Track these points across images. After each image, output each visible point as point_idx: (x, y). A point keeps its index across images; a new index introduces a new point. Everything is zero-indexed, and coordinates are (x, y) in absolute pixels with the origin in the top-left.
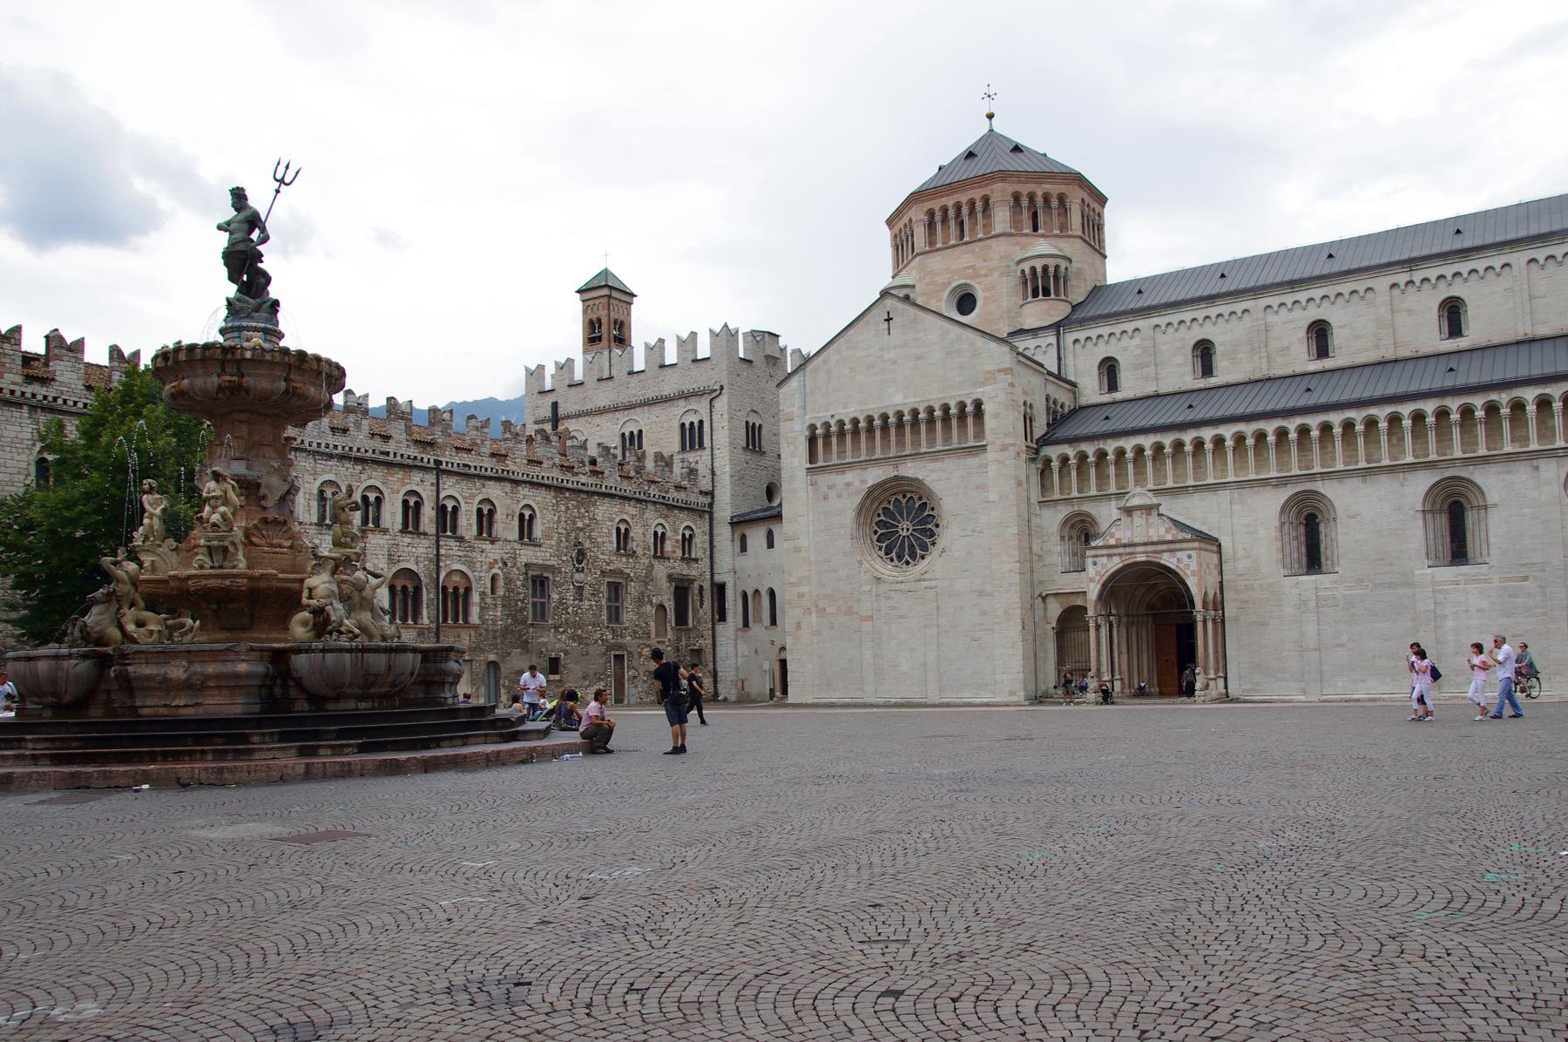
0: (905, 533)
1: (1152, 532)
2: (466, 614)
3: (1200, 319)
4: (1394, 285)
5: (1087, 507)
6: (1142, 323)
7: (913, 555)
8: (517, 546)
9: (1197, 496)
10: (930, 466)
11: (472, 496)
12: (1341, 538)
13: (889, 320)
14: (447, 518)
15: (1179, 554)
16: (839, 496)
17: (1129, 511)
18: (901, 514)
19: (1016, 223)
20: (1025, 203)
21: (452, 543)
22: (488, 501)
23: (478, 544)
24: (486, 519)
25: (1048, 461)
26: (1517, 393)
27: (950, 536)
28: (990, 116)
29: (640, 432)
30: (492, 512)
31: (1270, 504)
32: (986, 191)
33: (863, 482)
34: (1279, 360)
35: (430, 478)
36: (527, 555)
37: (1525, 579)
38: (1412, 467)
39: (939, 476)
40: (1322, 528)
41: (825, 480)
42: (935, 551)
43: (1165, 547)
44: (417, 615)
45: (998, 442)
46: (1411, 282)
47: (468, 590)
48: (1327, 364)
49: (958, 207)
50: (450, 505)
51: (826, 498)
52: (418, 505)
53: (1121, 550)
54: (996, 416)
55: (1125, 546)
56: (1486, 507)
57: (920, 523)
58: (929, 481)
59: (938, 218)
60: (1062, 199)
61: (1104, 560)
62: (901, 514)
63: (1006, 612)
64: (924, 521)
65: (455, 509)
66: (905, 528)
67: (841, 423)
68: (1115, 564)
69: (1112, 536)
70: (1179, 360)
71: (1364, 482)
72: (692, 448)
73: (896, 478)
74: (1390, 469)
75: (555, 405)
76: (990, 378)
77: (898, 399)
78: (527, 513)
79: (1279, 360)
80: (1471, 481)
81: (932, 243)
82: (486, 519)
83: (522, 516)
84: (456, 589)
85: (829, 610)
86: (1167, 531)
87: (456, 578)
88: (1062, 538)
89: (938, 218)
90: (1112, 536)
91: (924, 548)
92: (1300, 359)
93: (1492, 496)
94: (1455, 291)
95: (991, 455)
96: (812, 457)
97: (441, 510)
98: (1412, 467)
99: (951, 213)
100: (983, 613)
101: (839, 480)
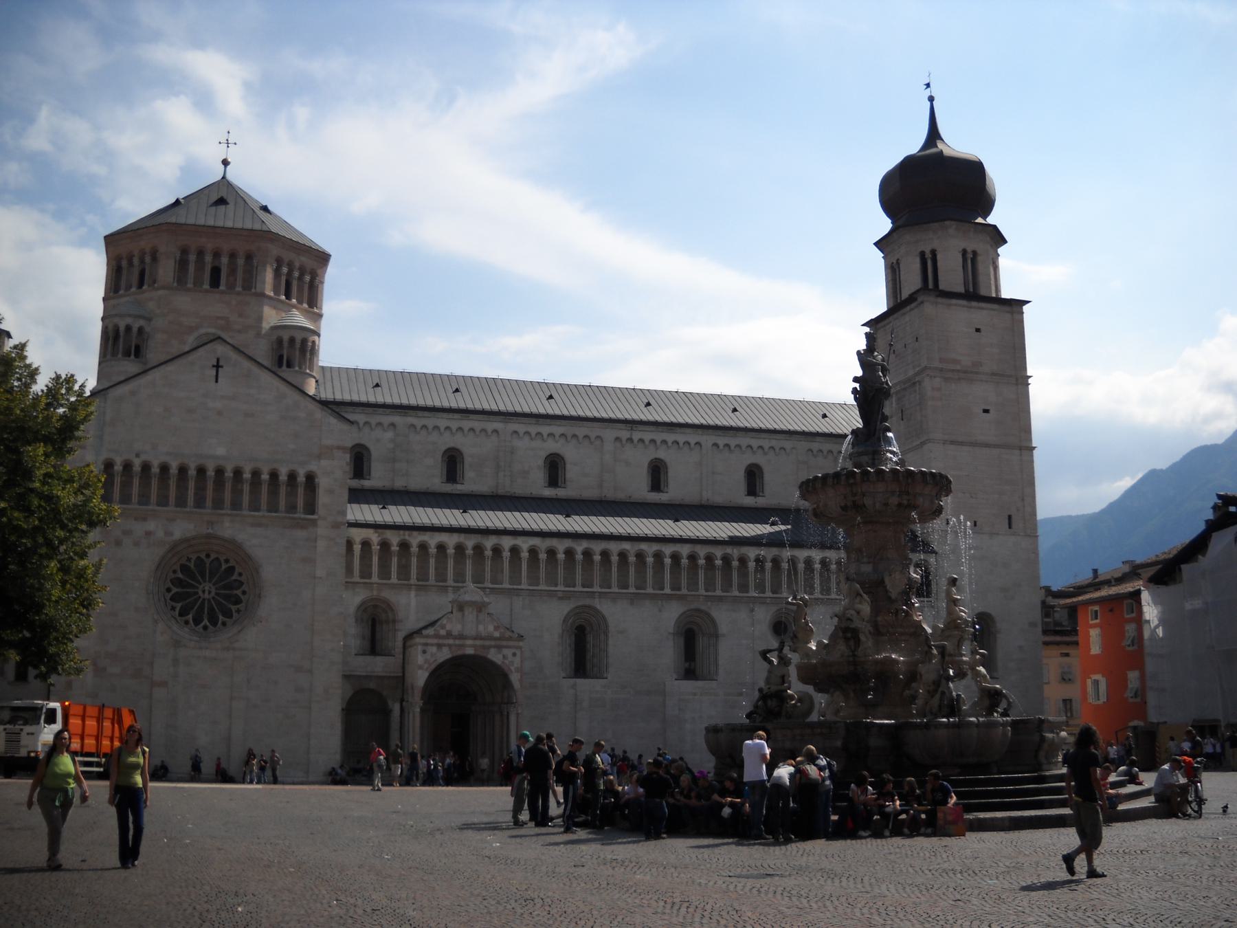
0: (206, 596)
1: (481, 628)
3: (454, 428)
4: (617, 439)
5: (387, 594)
6: (397, 419)
13: (217, 366)
15: (505, 651)
16: (137, 544)
18: (203, 576)
19: (276, 289)
20: (285, 270)
25: (350, 544)
28: (225, 163)
37: (741, 694)
38: (669, 597)
40: (590, 638)
43: (493, 643)
46: (630, 440)
49: (217, 255)
51: (118, 543)
53: (451, 641)
54: (331, 492)
55: (455, 638)
59: (192, 258)
61: (434, 649)
62: (203, 576)
66: (207, 590)
67: (146, 467)
68: (445, 655)
71: (632, 604)
73: (209, 536)
74: (653, 597)
77: (219, 450)
80: (708, 615)
81: (181, 278)
86: (496, 628)
88: (356, 621)
89: (192, 258)
90: (443, 627)
93: (723, 628)
94: (662, 454)
95: (322, 530)
99: (208, 258)
101: (139, 528)
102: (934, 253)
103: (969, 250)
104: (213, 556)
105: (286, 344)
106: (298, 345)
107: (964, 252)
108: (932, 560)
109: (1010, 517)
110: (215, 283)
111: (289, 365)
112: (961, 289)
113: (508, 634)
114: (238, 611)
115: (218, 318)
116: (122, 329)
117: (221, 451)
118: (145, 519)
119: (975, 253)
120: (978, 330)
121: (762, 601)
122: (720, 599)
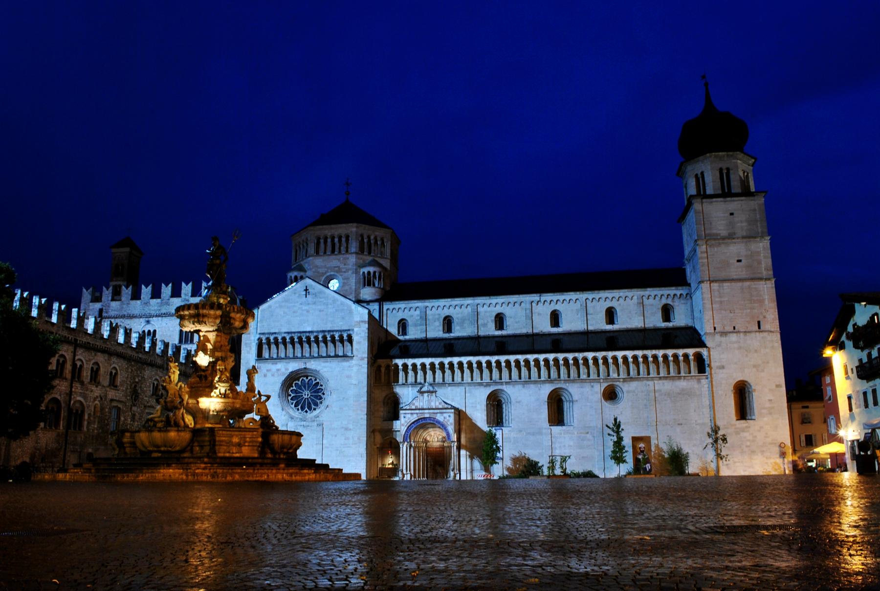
2: (81, 425)
7: (310, 408)
8: (108, 389)
9: (450, 388)
11: (90, 360)
12: (512, 412)
13: (306, 290)
14: (77, 372)
16: (273, 375)
17: (421, 393)
21: (78, 385)
22: (97, 363)
23: (90, 386)
24: (95, 373)
25: (380, 367)
26: (586, 354)
27: (329, 399)
29: (155, 331)
30: (98, 369)
31: (482, 394)
33: (287, 369)
35: (71, 348)
36: (112, 394)
38: (544, 382)
39: (326, 369)
40: (504, 406)
42: (322, 407)
44: (57, 425)
47: (83, 412)
48: (504, 333)
49: (333, 238)
50: (79, 363)
51: (265, 376)
52: (65, 362)
54: (359, 343)
57: (315, 392)
59: (322, 241)
60: (382, 240)
61: (409, 416)
63: (359, 439)
65: (81, 366)
66: (306, 394)
68: (415, 418)
70: (437, 323)
72: (186, 342)
74: (535, 382)
75: (101, 311)
78: (114, 372)
81: (317, 252)
82: (95, 373)
83: (111, 373)
84: (77, 411)
87: (77, 405)
88: (384, 403)
89: (322, 241)
91: (316, 404)
92: (489, 329)
93: (575, 398)
94: (557, 307)
95: (354, 362)
96: (260, 355)
97: (74, 365)
99: (329, 240)
102: (702, 173)
103: (724, 168)
107: (721, 170)
108: (704, 352)
109: (759, 323)
110: (333, 251)
111: (369, 285)
112: (720, 192)
113: (446, 406)
117: (309, 329)
119: (728, 169)
120: (732, 214)
121: (597, 381)
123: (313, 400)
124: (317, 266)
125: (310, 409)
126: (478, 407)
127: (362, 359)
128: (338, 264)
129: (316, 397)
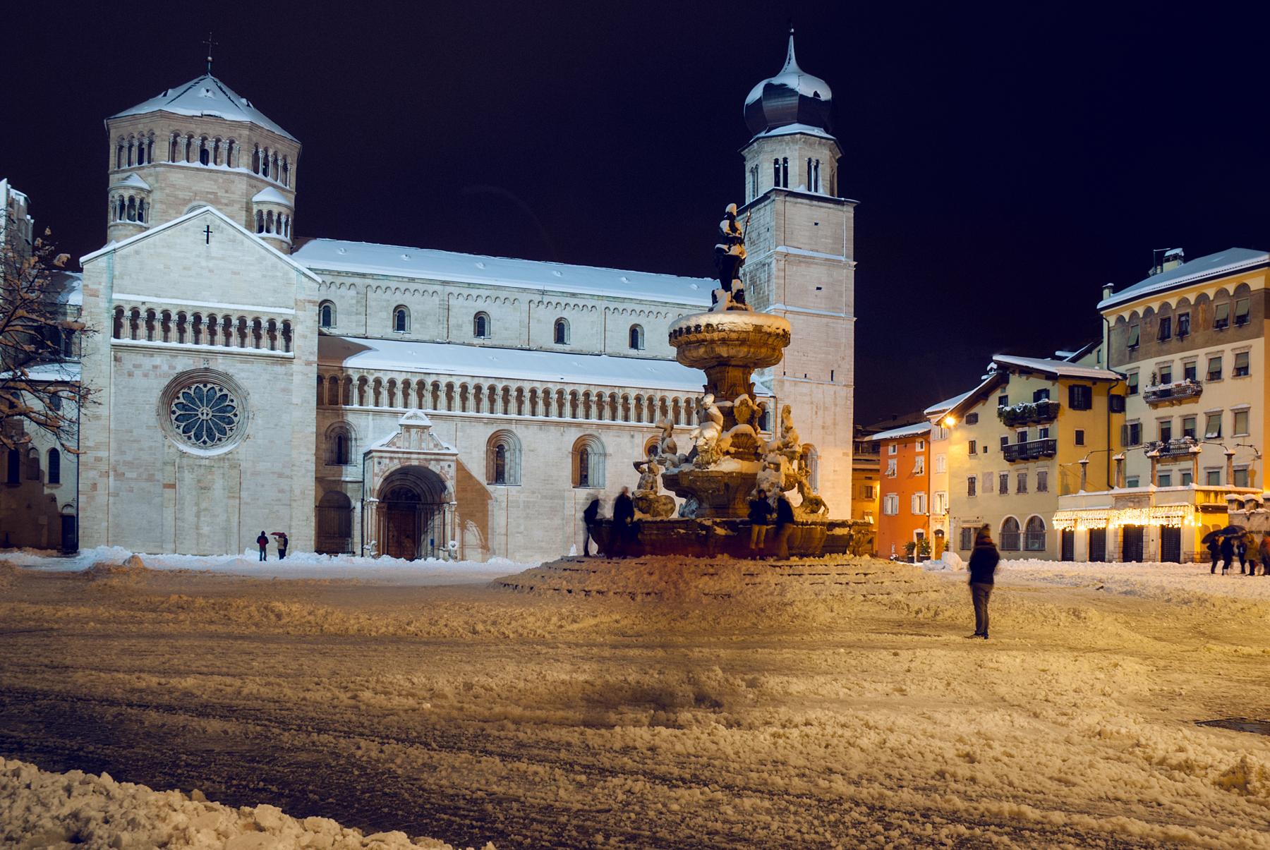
0: (205, 417)
1: (424, 445)
10: (240, 366)
16: (146, 375)
32: (235, 135)
33: (172, 367)
34: (455, 332)
41: (129, 359)
45: (304, 358)
51: (130, 375)
54: (305, 337)
56: (605, 455)
57: (219, 411)
58: (236, 377)
63: (303, 493)
64: (223, 410)
66: (205, 413)
68: (396, 465)
69: (394, 444)
70: (384, 315)
73: (206, 369)
76: (298, 304)
79: (455, 332)
80: (598, 438)
85: (128, 475)
93: (610, 450)
94: (565, 314)
95: (297, 366)
98: (570, 424)
100: (281, 491)
101: (147, 362)
104: (209, 386)
105: (265, 217)
106: (275, 218)
114: (231, 429)
115: (208, 193)
116: (126, 199)
118: (152, 356)
121: (640, 429)
122: (608, 427)
123: (215, 424)
124: (173, 186)
125: (212, 440)
126: (475, 453)
127: (308, 363)
128: (214, 188)
129: (222, 419)
